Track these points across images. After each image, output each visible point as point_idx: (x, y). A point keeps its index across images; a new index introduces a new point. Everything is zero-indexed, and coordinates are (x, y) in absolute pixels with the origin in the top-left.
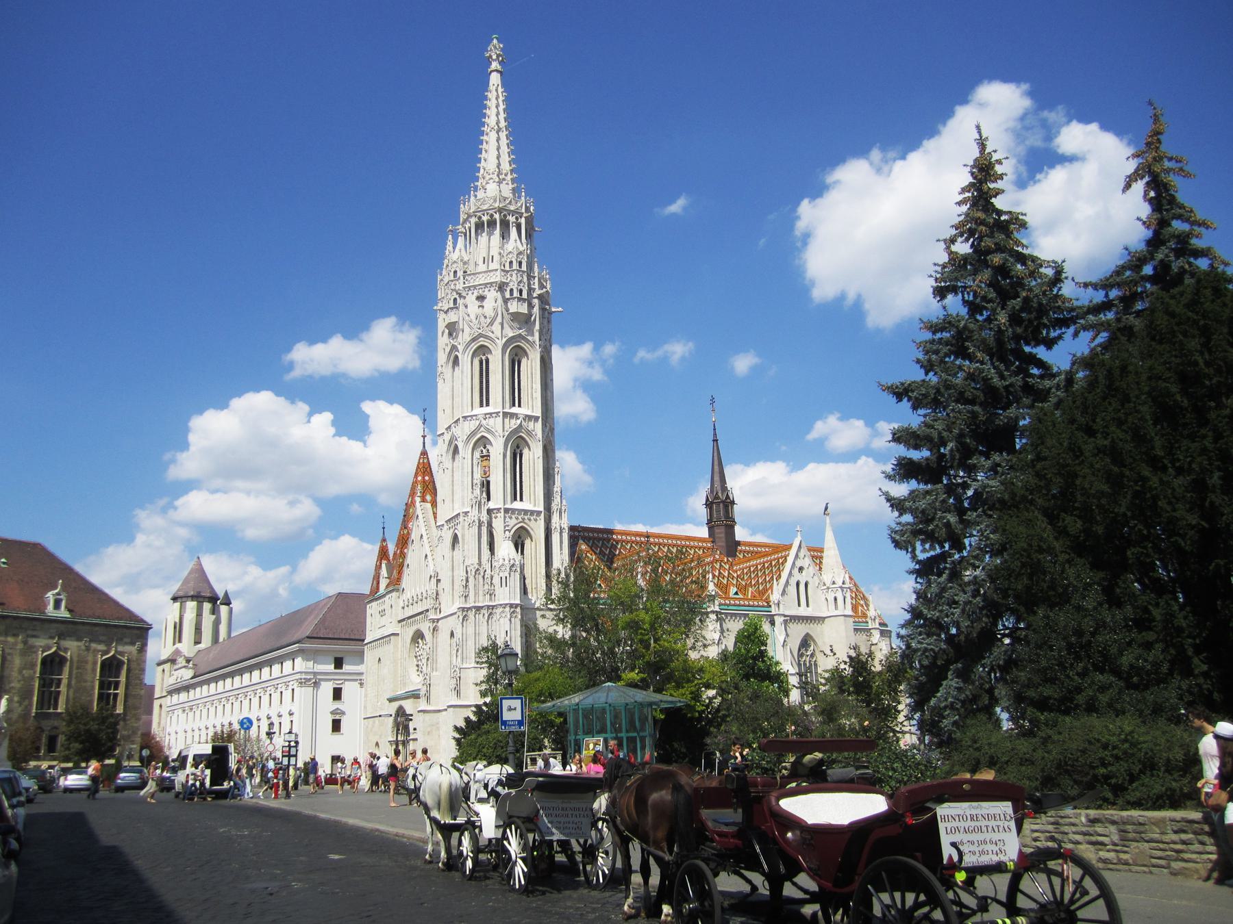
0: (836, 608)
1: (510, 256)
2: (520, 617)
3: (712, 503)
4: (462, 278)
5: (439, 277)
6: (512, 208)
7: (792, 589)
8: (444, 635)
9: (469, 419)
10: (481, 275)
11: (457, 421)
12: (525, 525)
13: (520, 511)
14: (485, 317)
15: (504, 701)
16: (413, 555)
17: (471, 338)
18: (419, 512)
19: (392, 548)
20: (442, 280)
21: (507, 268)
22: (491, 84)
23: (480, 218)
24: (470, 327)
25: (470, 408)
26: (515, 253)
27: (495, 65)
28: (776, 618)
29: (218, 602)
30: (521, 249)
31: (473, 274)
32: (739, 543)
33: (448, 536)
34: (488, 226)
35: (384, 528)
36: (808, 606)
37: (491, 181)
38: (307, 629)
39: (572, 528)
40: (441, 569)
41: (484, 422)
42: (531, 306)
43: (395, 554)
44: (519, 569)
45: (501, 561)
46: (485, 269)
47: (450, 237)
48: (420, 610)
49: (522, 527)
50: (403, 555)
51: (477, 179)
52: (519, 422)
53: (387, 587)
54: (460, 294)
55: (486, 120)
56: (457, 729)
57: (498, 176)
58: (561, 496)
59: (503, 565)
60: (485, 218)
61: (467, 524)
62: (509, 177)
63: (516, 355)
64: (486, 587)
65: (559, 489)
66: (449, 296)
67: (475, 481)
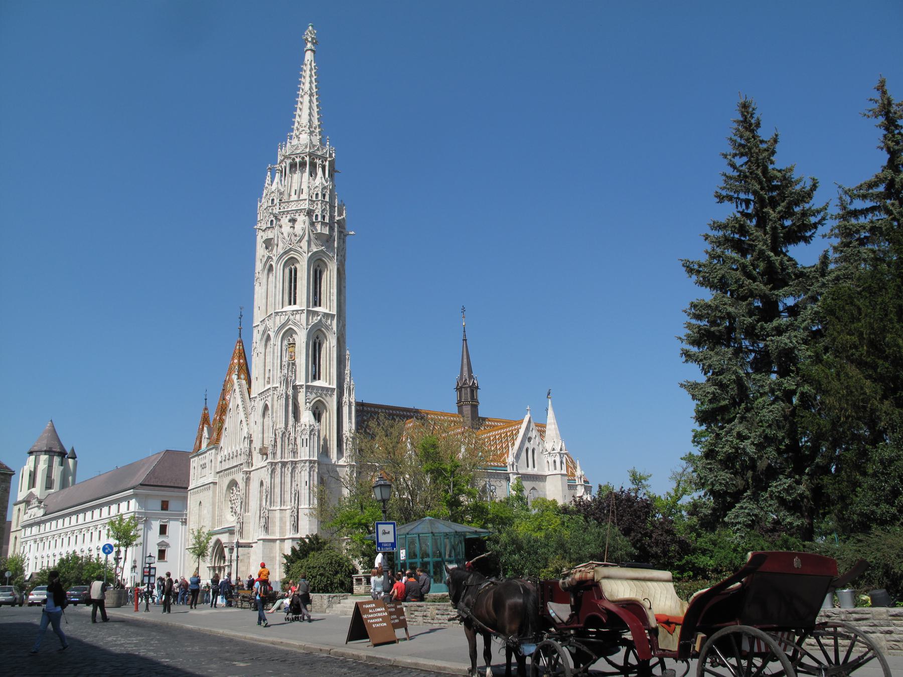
0: (555, 469)
1: (317, 189)
2: (317, 470)
3: (461, 387)
4: (278, 204)
5: (259, 204)
6: (319, 153)
7: (524, 454)
8: (254, 485)
9: (280, 314)
10: (293, 203)
12: (322, 400)
15: (392, 525)
16: (229, 422)
18: (236, 387)
19: (213, 416)
20: (261, 206)
21: (314, 199)
22: (306, 60)
23: (294, 159)
24: (283, 243)
25: (281, 306)
27: (309, 45)
28: (511, 475)
29: (66, 456)
30: (326, 185)
31: (287, 202)
32: (484, 419)
33: (259, 406)
34: (300, 166)
35: (206, 399)
36: (534, 467)
37: (303, 132)
38: (140, 477)
39: (357, 404)
40: (254, 432)
41: (291, 317)
42: (332, 229)
43: (215, 420)
44: (317, 434)
45: (303, 426)
46: (296, 199)
48: (235, 464)
49: (319, 400)
50: (222, 421)
51: (292, 130)
52: (319, 318)
53: (208, 445)
54: (276, 217)
55: (302, 86)
56: (286, 557)
57: (309, 128)
58: (350, 377)
59: (304, 429)
60: (298, 160)
61: (276, 397)
62: (318, 130)
63: (318, 266)
64: (291, 446)
66: (267, 218)
67: (284, 363)
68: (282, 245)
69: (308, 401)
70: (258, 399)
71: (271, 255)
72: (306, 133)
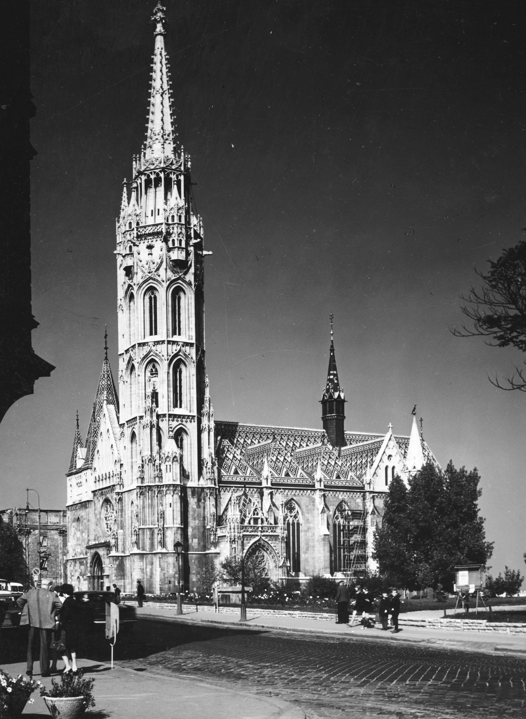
1: (172, 211)
4: (135, 229)
5: (117, 225)
10: (150, 228)
11: (133, 347)
13: (179, 416)
14: (154, 263)
17: (143, 280)
22: (156, 47)
24: (142, 271)
26: (176, 209)
27: (159, 28)
33: (128, 432)
37: (157, 141)
41: (154, 348)
42: (188, 254)
47: (125, 189)
49: (181, 428)
51: (146, 138)
57: (162, 137)
58: (209, 404)
59: (168, 456)
60: (153, 177)
62: (171, 137)
65: (208, 399)
68: (142, 273)
69: (170, 429)
70: (126, 426)
71: (132, 284)
72: (159, 142)
